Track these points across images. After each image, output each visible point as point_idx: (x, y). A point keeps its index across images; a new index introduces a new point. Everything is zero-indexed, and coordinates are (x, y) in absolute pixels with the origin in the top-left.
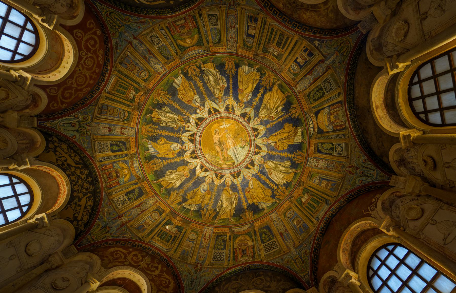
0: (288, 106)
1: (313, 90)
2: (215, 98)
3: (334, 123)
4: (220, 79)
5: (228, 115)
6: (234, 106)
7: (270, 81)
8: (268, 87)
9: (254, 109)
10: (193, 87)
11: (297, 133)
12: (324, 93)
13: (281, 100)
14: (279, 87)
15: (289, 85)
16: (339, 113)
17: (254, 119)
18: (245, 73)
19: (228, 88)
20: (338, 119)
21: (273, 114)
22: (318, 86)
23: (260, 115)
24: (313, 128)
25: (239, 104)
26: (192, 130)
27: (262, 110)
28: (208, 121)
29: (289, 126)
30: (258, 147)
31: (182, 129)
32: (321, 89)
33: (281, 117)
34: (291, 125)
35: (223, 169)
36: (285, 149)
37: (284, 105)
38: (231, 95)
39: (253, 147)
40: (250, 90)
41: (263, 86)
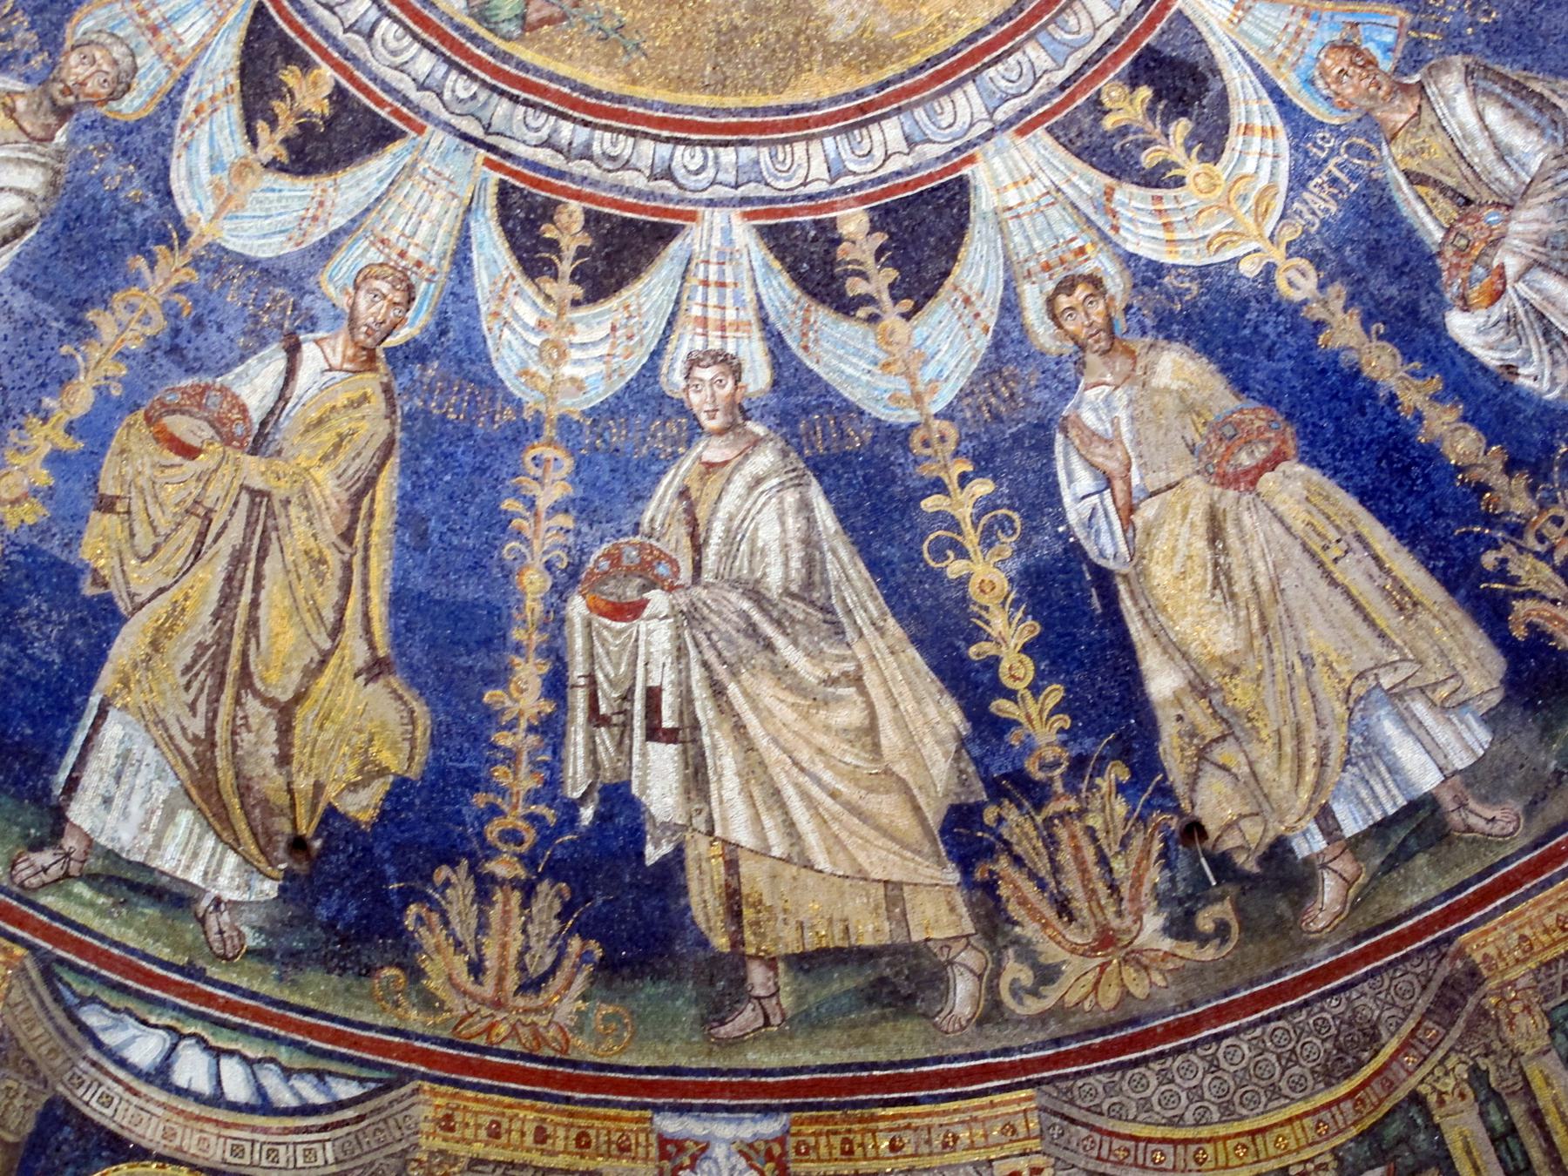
2: (1454, 42)
6: (1130, 197)
7: (1063, 907)
8: (1015, 823)
9: (898, 436)
11: (216, 815)
13: (753, 874)
18: (1395, 695)
19: (1414, 327)
21: (655, 633)
23: (764, 459)
24: (160, 1075)
25: (1117, 284)
27: (810, 542)
29: (370, 772)
33: (552, 730)
34: (362, 805)
36: (100, 523)
37: (676, 861)
38: (1299, 283)
40: (1161, 574)
41: (1078, 765)
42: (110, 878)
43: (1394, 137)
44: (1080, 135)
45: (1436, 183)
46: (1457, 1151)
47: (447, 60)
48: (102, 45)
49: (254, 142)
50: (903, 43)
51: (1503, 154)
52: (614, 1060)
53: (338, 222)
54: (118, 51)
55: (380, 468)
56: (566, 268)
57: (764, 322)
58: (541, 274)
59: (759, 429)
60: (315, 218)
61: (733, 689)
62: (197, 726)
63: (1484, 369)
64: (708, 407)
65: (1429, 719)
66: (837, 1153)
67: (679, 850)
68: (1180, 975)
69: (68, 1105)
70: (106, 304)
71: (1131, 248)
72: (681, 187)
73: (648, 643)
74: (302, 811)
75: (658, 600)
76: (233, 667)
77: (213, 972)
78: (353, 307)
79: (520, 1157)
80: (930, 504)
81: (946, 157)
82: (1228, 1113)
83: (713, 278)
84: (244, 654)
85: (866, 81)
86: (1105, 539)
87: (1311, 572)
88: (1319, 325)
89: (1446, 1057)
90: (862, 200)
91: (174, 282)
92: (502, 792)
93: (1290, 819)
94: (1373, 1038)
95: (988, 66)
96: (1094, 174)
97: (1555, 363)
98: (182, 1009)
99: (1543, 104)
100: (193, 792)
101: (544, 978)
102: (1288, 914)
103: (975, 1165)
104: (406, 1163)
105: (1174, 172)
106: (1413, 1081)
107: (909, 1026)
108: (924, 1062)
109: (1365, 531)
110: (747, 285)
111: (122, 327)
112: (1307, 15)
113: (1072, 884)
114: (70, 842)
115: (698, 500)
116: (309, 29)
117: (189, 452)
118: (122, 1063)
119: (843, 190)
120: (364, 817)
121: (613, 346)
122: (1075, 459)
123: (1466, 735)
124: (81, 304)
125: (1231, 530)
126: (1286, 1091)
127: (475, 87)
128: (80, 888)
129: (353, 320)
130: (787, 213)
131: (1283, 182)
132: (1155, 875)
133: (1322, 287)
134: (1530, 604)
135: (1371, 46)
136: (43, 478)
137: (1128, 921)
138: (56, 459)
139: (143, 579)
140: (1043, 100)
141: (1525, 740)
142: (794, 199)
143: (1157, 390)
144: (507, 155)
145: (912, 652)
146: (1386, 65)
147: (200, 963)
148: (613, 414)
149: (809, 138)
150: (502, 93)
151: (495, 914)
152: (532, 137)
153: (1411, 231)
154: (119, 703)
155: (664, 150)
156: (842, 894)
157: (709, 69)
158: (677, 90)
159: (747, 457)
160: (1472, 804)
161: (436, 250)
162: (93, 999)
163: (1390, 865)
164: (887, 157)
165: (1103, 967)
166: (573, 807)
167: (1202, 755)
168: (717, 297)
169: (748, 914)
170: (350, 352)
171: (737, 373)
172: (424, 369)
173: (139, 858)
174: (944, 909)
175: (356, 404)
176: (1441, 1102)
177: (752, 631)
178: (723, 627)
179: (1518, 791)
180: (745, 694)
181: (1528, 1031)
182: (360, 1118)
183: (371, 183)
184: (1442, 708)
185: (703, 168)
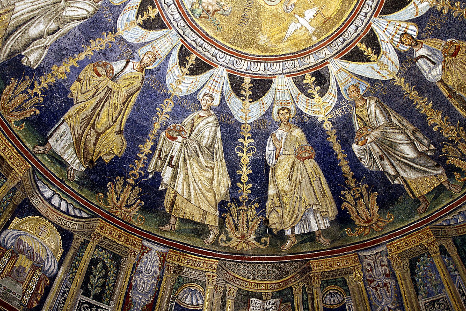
0: (152, 195)
1: (116, 280)
2: (376, 94)
3: (12, 258)
4: (382, 158)
5: (311, 60)
6: (302, 97)
7: (237, 227)
8: (233, 208)
9: (239, 124)
10: (454, 103)
11: (78, 151)
12: (87, 293)
13: (179, 199)
14: (205, 226)
15: (182, 248)
16: (19, 289)
17: (223, 97)
18: (315, 211)
19: (346, 144)
20: (9, 275)
21: (177, 145)
22: (111, 299)
23: (211, 119)
24: (49, 200)
25: (293, 112)
29: (111, 153)
30: (156, 24)
32: (98, 298)
33: (150, 157)
34: (107, 159)
36: (76, 83)
38: (328, 126)
40: (279, 170)
41: (250, 201)
42: (52, 156)
43: (357, 107)
44: (298, 81)
45: (361, 119)
46: (295, 301)
47: (182, 17)
50: (272, 50)
51: (376, 119)
52: (139, 226)
53: (148, 41)
55: (135, 92)
56: (188, 67)
57: (222, 92)
60: (143, 38)
61: (188, 162)
62: (80, 131)
63: (356, 157)
65: (319, 218)
66: (176, 260)
67: (166, 189)
68: (254, 249)
69: (29, 200)
70: (95, 40)
71: (299, 107)
73: (175, 146)
74: (95, 156)
75: (180, 139)
76: (92, 122)
77: (66, 182)
79: (114, 239)
80: (240, 140)
81: (271, 75)
82: (254, 278)
83: (216, 80)
84: (95, 120)
85: (261, 54)
86: (271, 160)
87: (308, 181)
88: (328, 136)
89: (299, 282)
90: (251, 76)
91: (110, 40)
92: (136, 166)
93: (286, 227)
94: (287, 274)
95: (286, 61)
96: (297, 89)
97: (369, 161)
98: (58, 188)
99: (388, 113)
100: (75, 145)
101: (131, 205)
102: (279, 244)
103: (202, 271)
104: (91, 233)
105: (313, 96)
106: (292, 284)
107: (198, 240)
108: (199, 248)
109: (321, 178)
110: (222, 84)
111: (96, 45)
112: (351, 78)
113: (240, 224)
114: (47, 147)
117: (99, 75)
118: (42, 195)
120: (106, 161)
122: (271, 142)
123: (325, 223)
124: (90, 38)
125: (296, 167)
126: (267, 278)
127: (185, 24)
128: (46, 156)
129: (142, 61)
130: (235, 73)
131: (333, 106)
132: (256, 228)
133: (332, 129)
134: (347, 203)
135: (360, 89)
136: (69, 70)
137: (248, 235)
138: (73, 67)
139: (81, 98)
140: (294, 72)
141: (336, 229)
142: (238, 71)
143: (292, 135)
144: (186, 40)
145: (226, 167)
146: (362, 93)
147: (64, 180)
149: (245, 60)
150: (190, 28)
151: (125, 189)
152: (192, 39)
153: (353, 126)
154: (67, 121)
155: (217, 51)
156: (195, 210)
157: (232, 40)
160: (321, 237)
161: (164, 53)
162: (41, 180)
163: (301, 243)
165: (240, 242)
166: (148, 174)
167: (274, 208)
168: (214, 83)
169: (175, 207)
170: (139, 67)
171: (213, 100)
172: (152, 76)
173: (60, 155)
174: (214, 219)
175: (135, 77)
176: (296, 290)
177: (196, 151)
178: (190, 149)
179: (331, 238)
180: (190, 163)
181: (317, 283)
182: (86, 222)
183: (157, 35)
184: (323, 217)
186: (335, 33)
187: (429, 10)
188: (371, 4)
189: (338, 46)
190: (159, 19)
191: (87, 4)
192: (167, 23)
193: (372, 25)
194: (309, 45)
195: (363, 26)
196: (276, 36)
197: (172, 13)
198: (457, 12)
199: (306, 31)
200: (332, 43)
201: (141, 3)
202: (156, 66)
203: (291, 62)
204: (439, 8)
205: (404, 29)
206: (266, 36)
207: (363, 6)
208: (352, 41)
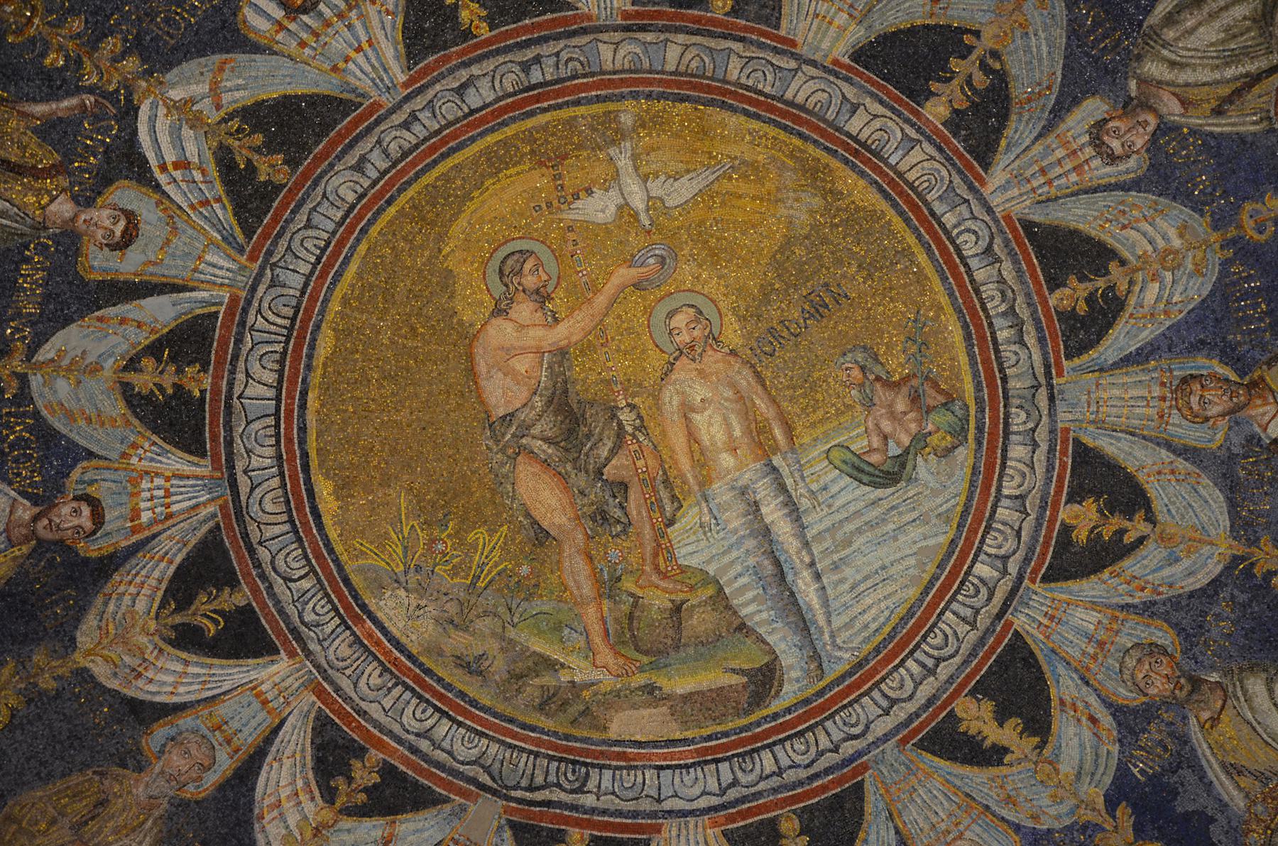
5: (676, 53)
17: (1060, 111)
23: (1153, 69)
26: (173, 270)
28: (397, 140)
31: (31, 277)
35: (625, 756)
39: (1026, 471)
48: (1132, 675)
49: (1141, 540)
50: (791, 156)
53: (1164, 452)
54: (1130, 662)
58: (1116, 298)
59: (1133, 84)
60: (1173, 472)
64: (1141, 130)
72: (992, 238)
78: (1223, 415)
81: (847, 79)
85: (835, 164)
90: (917, 114)
95: (766, 96)
115: (1218, 98)
116: (1041, 540)
119: (919, 130)
121: (1137, 221)
127: (1014, 410)
129: (1231, 412)
130: (961, 156)
140: (761, 46)
142: (949, 159)
144: (1047, 367)
148: (1189, 195)
149: (900, 175)
152: (1023, 355)
155: (974, 263)
158: (927, 278)
159: (1159, 82)
164: (876, 116)
168: (1052, 168)
170: (1259, 402)
172: (1239, 344)
185: (968, 230)
186: (545, 105)
187: (169, 66)
188: (377, 152)
189: (557, 54)
190: (1081, 486)
191: (1251, 709)
192: (1064, 453)
193: (402, 78)
194: (659, 106)
195: (438, 87)
196: (752, 192)
197: (1026, 470)
198: (63, 32)
199: (644, 157)
200: (574, 77)
201: (1095, 572)
202: (1201, 361)
203: (750, 83)
204: (131, 64)
205: (292, 26)
206: (783, 211)
207: (405, 155)
208: (498, 52)
